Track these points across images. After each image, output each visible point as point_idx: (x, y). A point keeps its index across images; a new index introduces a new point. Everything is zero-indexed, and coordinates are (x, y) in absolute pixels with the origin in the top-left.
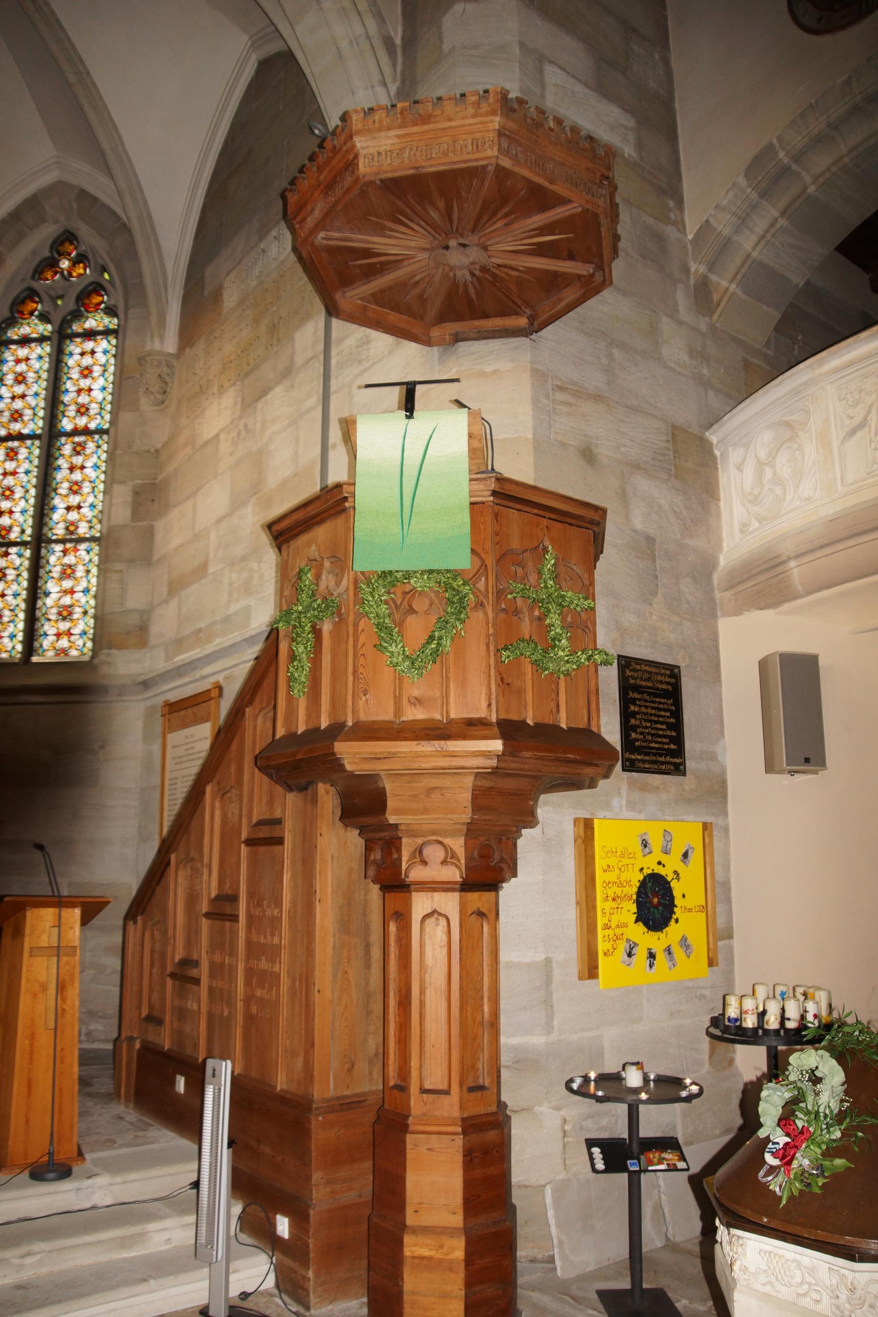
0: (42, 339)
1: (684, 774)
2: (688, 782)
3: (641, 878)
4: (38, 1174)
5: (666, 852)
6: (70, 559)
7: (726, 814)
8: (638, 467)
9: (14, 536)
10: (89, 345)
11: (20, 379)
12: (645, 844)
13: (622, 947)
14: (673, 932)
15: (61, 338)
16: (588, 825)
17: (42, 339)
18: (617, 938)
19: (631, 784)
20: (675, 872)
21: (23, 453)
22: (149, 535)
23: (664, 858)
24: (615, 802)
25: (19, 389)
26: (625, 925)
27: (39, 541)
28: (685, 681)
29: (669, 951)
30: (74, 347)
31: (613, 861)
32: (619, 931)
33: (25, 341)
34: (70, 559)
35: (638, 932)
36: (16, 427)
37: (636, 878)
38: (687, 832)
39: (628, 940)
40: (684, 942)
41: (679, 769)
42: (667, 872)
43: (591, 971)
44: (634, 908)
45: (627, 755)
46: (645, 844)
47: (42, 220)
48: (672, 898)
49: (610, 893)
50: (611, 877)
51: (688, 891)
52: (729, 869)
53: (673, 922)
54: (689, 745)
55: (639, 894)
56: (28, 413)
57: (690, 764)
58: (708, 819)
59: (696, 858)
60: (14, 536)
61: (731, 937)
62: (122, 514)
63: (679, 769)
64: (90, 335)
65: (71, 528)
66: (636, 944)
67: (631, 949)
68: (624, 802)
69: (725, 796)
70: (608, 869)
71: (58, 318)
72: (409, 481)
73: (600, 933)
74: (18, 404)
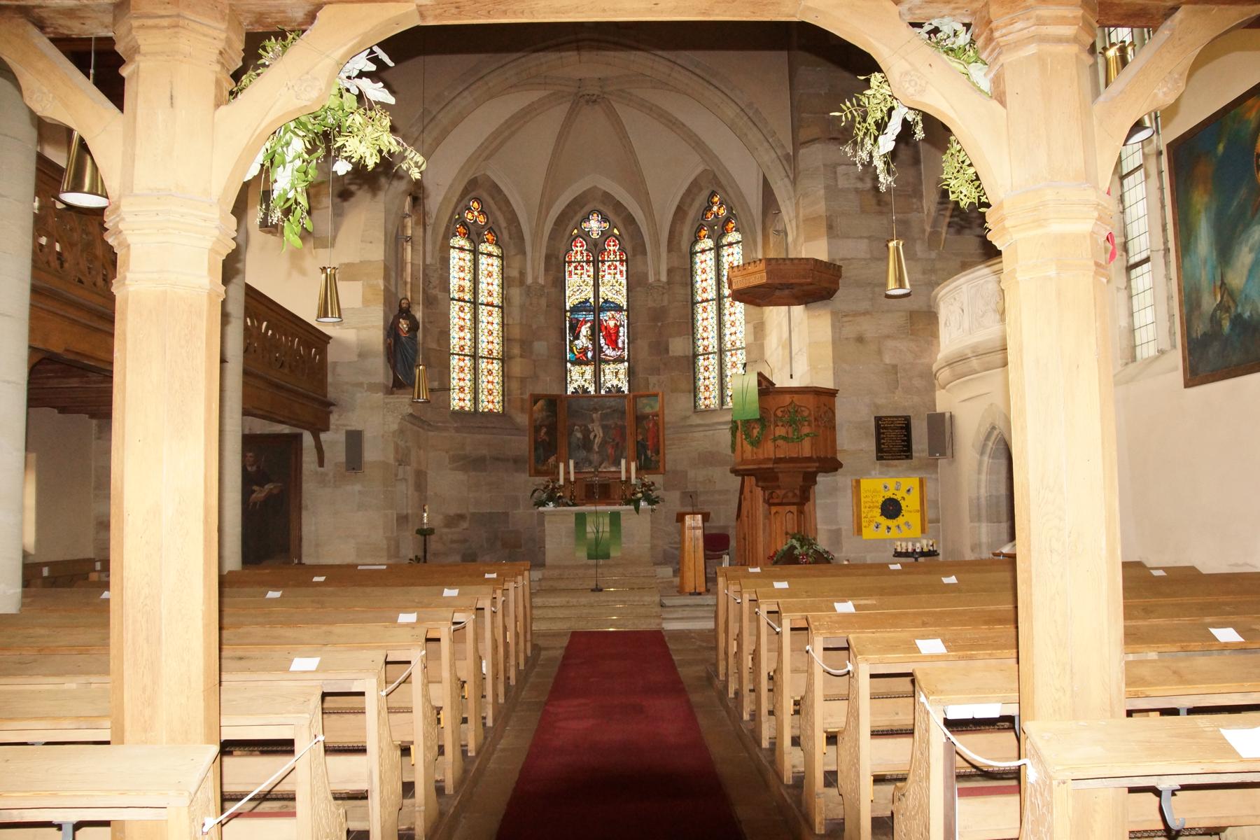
0: (710, 249)
2: (914, 462)
4: (691, 594)
6: (734, 359)
8: (888, 337)
9: (710, 349)
10: (730, 251)
11: (704, 271)
14: (900, 520)
15: (718, 248)
16: (858, 482)
17: (710, 249)
19: (881, 465)
21: (709, 308)
22: (762, 347)
25: (704, 276)
27: (721, 352)
28: (912, 421)
30: (725, 251)
33: (703, 251)
34: (734, 359)
36: (705, 296)
37: (881, 500)
38: (913, 482)
40: (907, 524)
41: (909, 457)
42: (898, 497)
43: (859, 531)
47: (701, 189)
51: (910, 504)
54: (914, 447)
56: (709, 289)
59: (916, 493)
60: (710, 349)
62: (751, 339)
63: (909, 457)
64: (730, 245)
65: (733, 344)
71: (716, 235)
72: (744, 392)
74: (704, 284)
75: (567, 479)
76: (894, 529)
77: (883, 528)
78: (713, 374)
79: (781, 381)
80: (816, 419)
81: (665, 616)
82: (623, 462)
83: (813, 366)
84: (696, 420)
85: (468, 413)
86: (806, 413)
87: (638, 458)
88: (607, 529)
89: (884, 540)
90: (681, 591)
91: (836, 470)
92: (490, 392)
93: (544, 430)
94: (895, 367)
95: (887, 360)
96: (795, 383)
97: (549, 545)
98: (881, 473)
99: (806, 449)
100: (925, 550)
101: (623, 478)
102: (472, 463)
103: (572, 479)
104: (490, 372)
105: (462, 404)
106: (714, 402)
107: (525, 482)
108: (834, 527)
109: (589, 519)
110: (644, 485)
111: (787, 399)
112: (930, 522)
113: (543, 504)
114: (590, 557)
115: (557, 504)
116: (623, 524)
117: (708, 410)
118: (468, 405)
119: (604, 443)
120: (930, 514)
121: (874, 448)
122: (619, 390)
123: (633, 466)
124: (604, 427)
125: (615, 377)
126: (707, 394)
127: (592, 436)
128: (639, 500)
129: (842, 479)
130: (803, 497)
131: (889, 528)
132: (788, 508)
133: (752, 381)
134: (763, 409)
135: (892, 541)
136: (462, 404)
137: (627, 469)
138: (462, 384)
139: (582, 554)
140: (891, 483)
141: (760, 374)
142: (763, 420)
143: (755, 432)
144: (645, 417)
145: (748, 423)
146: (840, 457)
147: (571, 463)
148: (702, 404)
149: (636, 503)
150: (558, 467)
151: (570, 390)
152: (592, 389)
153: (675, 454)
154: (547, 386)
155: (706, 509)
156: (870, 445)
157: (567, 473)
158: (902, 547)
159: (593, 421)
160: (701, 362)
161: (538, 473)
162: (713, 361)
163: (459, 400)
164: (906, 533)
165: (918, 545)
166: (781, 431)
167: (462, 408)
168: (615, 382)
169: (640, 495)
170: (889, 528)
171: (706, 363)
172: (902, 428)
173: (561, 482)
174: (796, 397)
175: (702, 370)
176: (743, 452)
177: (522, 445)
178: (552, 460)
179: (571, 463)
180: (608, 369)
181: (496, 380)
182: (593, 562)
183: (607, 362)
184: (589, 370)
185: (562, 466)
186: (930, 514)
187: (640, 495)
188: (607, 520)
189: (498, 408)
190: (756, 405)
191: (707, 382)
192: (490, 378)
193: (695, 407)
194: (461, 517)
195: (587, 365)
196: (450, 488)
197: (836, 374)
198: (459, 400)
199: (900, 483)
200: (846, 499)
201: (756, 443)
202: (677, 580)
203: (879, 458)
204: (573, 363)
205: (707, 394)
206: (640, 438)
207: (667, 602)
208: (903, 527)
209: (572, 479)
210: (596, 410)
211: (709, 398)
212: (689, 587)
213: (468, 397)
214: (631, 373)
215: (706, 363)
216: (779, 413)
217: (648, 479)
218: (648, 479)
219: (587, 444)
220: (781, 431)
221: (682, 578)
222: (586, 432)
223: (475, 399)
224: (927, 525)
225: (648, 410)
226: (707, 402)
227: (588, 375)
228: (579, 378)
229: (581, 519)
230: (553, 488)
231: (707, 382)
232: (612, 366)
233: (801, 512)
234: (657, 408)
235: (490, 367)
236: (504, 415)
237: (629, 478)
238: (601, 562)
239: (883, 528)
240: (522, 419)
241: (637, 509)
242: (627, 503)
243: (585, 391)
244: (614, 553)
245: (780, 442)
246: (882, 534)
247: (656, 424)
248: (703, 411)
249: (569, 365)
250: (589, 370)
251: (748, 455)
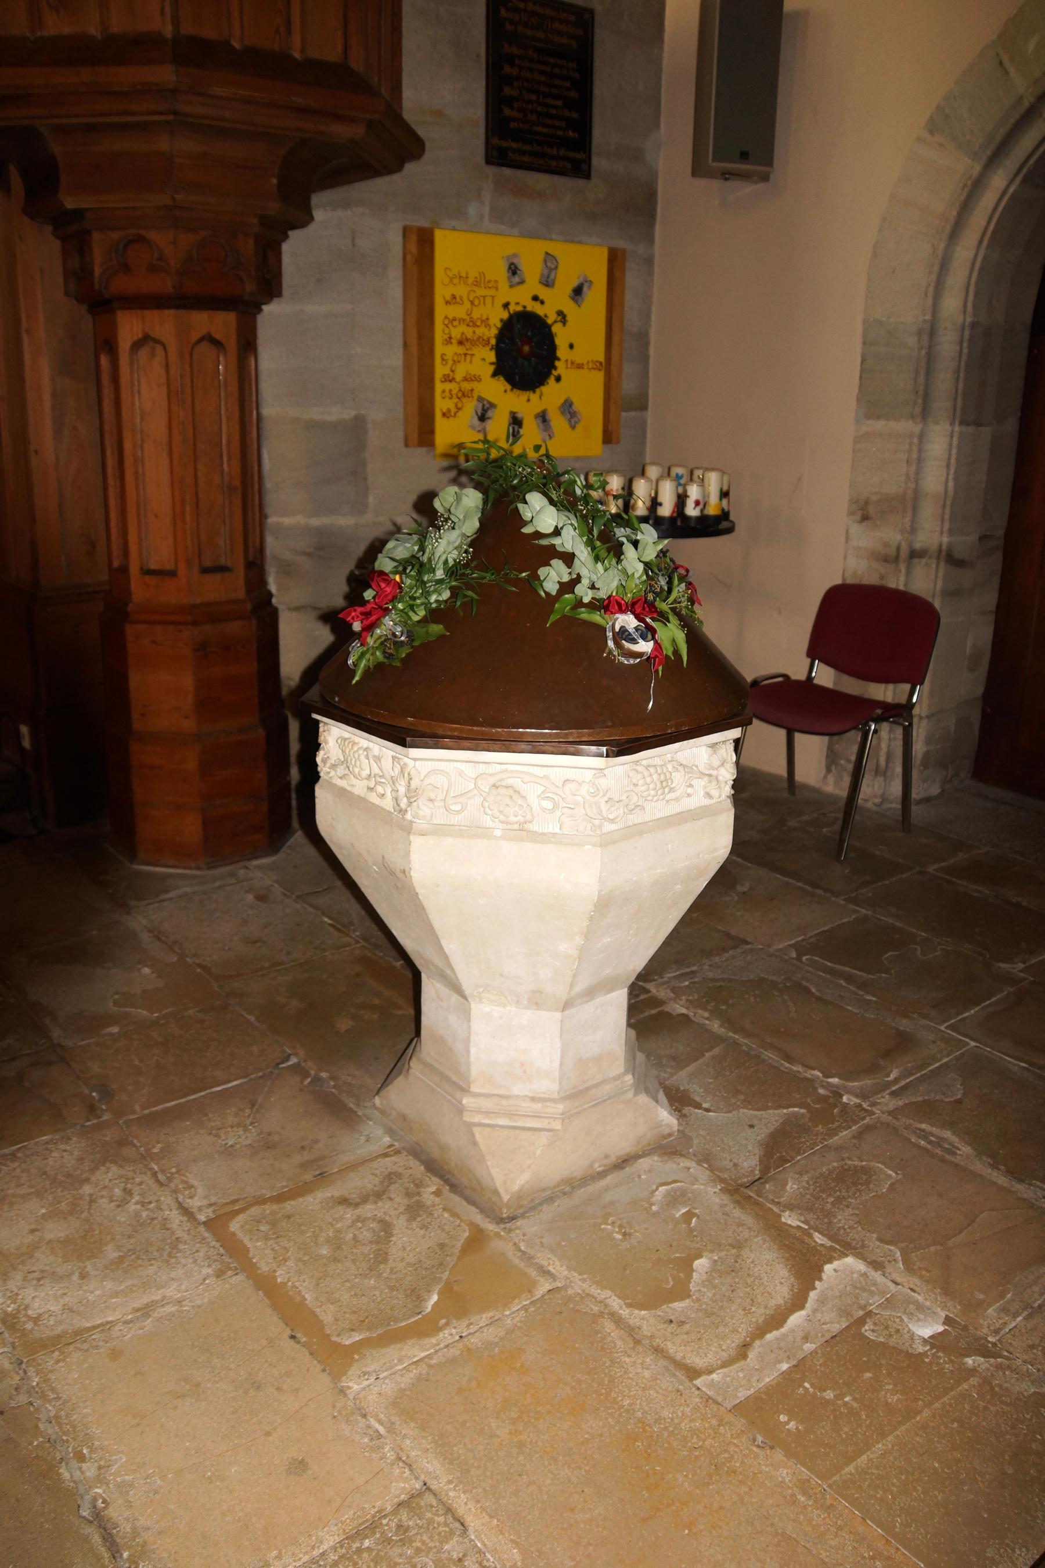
1: (587, 176)
2: (594, 189)
3: (505, 315)
5: (547, 282)
7: (651, 240)
12: (514, 270)
13: (470, 408)
14: (551, 395)
18: (464, 395)
20: (560, 313)
23: (543, 292)
24: (472, 210)
26: (477, 379)
29: (543, 417)
31: (461, 291)
32: (467, 386)
35: (496, 390)
37: (497, 316)
38: (585, 259)
39: (480, 399)
40: (568, 409)
41: (581, 169)
42: (548, 312)
44: (492, 356)
45: (495, 141)
46: (514, 270)
48: (553, 347)
49: (456, 333)
50: (458, 311)
51: (579, 337)
52: (648, 316)
53: (552, 380)
54: (597, 134)
55: (501, 337)
57: (598, 163)
58: (620, 244)
59: (597, 297)
61: (643, 407)
63: (581, 169)
66: (492, 406)
67: (485, 411)
68: (486, 210)
69: (652, 216)
70: (453, 300)
73: (439, 387)
98: (498, 216)
108: (336, 413)
121: (478, 112)
132: (202, 321)
140: (531, 254)
165: (694, 492)
208: (558, 422)
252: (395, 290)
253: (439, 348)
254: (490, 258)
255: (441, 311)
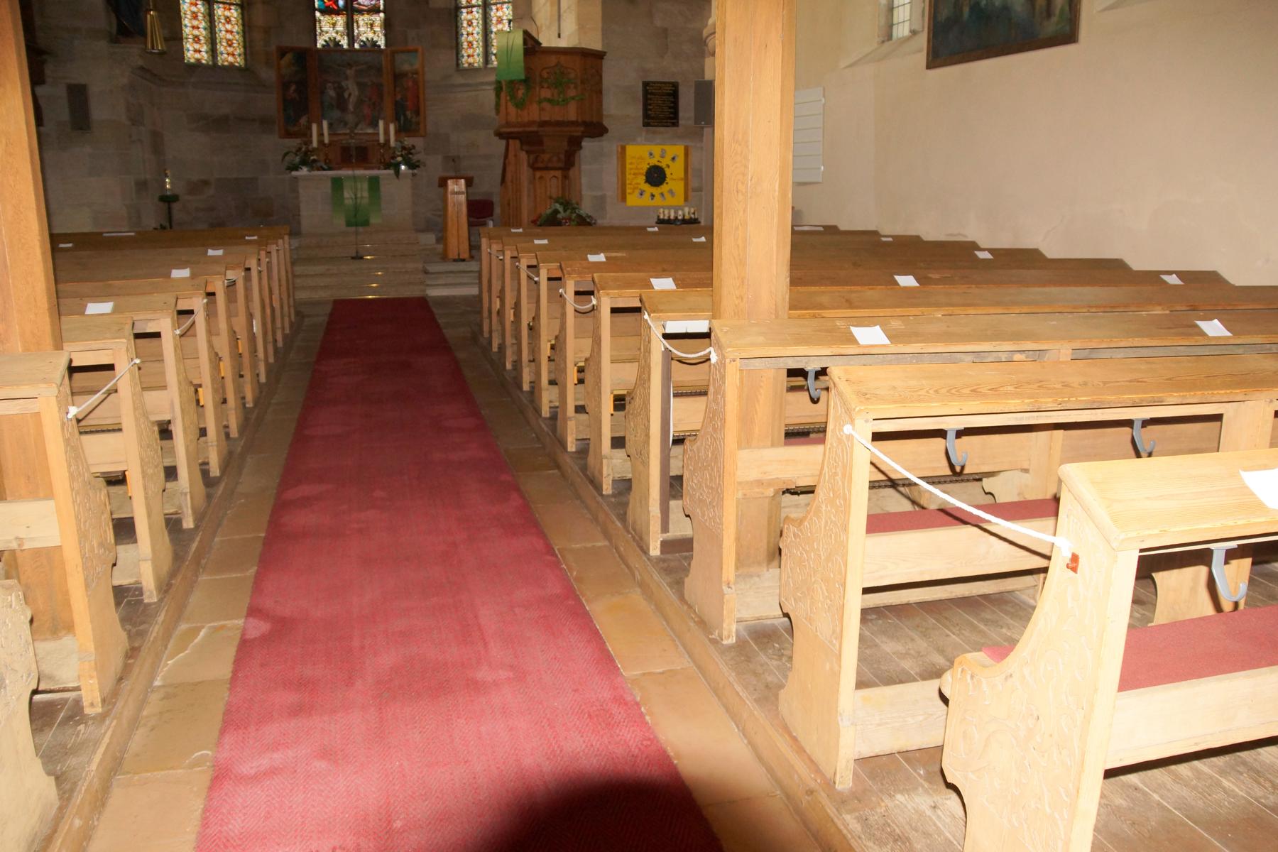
2: (680, 130)
4: (455, 260)
6: (500, 13)
13: (637, 192)
14: (664, 188)
16: (623, 149)
29: (662, 194)
34: (500, 13)
35: (649, 189)
37: (645, 167)
38: (678, 150)
40: (671, 192)
41: (675, 124)
42: (663, 165)
43: (624, 198)
51: (675, 172)
54: (681, 114)
63: (675, 124)
75: (321, 142)
76: (658, 197)
77: (647, 195)
78: (477, 30)
79: (547, 39)
80: (582, 82)
81: (429, 282)
82: (381, 123)
83: (581, 27)
84: (459, 80)
85: (206, 67)
86: (572, 76)
87: (397, 119)
88: (366, 194)
89: (648, 208)
90: (444, 257)
91: (601, 135)
92: (230, 44)
93: (293, 88)
94: (665, 30)
95: (658, 23)
96: (563, 43)
97: (304, 213)
99: (572, 113)
100: (687, 217)
101: (382, 139)
102: (217, 124)
103: (326, 140)
104: (228, 20)
105: (197, 56)
106: (477, 60)
107: (273, 145)
108: (599, 193)
109: (347, 184)
110: (404, 148)
111: (553, 60)
112: (694, 190)
113: (296, 168)
114: (349, 224)
115: (312, 165)
116: (382, 189)
117: (472, 70)
118: (204, 57)
119: (360, 102)
120: (694, 183)
121: (641, 113)
122: (374, 44)
123: (392, 127)
124: (359, 85)
125: (371, 30)
126: (470, 51)
127: (346, 95)
128: (398, 165)
129: (607, 145)
130: (568, 162)
131: (653, 196)
132: (552, 173)
133: (518, 39)
134: (528, 69)
135: (658, 207)
136: (197, 56)
137: (386, 131)
138: (196, 32)
139: (340, 222)
140: (657, 150)
141: (526, 33)
142: (526, 81)
143: (521, 93)
144: (404, 75)
145: (512, 83)
146: (606, 123)
147: (325, 124)
148: (465, 61)
149: (397, 166)
150: (310, 128)
151: (320, 43)
152: (344, 43)
153: (437, 115)
154: (296, 40)
155: (470, 174)
156: (636, 111)
157: (321, 134)
158: (664, 214)
159: (347, 78)
160: (464, 15)
161: (288, 135)
162: (477, 14)
163: (195, 51)
164: (670, 201)
165: (680, 212)
166: (546, 93)
167: (198, 60)
168: (370, 35)
169: (399, 159)
170: (653, 196)
171: (469, 17)
172: (669, 95)
173: (315, 144)
174: (563, 58)
175: (465, 24)
176: (507, 114)
177: (269, 103)
178: (303, 121)
179: (325, 124)
180: (362, 20)
181: (236, 29)
182: (353, 229)
183: (361, 12)
184: (340, 20)
185: (314, 127)
186: (694, 183)
187: (399, 159)
188: (366, 186)
189: (239, 61)
190: (522, 64)
191: (470, 38)
192: (229, 27)
193: (458, 65)
194: (205, 183)
195: (338, 12)
196: (192, 154)
197: (605, 33)
198: (195, 51)
199: (668, 152)
200: (612, 165)
201: (520, 105)
202: (440, 247)
203: (646, 125)
204: (323, 12)
205: (470, 51)
206: (399, 97)
207: (431, 268)
209: (326, 140)
210: (350, 65)
211: (472, 55)
212: (453, 254)
213: (204, 48)
214: (387, 25)
215: (469, 17)
216: (545, 75)
217: (408, 142)
218: (408, 142)
219: (341, 104)
220: (546, 93)
221: (446, 245)
222: (340, 90)
223: (213, 51)
224: (690, 194)
225: (406, 67)
226: (471, 60)
227: (340, 28)
228: (330, 29)
229: (337, 184)
230: (306, 153)
231: (470, 38)
232: (366, 17)
233: (566, 177)
234: (417, 66)
235: (227, 13)
236: (245, 71)
237: (387, 141)
238: (361, 229)
239: (647, 195)
240: (268, 75)
241: (397, 172)
242: (387, 167)
243: (337, 44)
244: (374, 220)
245: (546, 105)
246: (646, 201)
247: (416, 83)
248: (466, 70)
249: (318, 14)
250: (340, 20)
251: (513, 118)
252: (615, 161)
253: (628, 176)
254: (642, 153)
255: (628, 166)
